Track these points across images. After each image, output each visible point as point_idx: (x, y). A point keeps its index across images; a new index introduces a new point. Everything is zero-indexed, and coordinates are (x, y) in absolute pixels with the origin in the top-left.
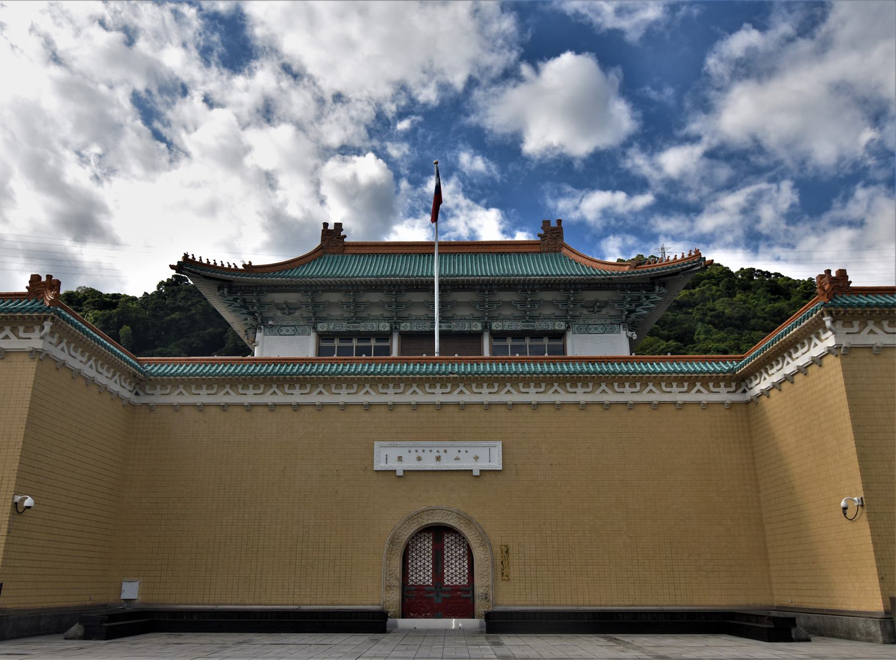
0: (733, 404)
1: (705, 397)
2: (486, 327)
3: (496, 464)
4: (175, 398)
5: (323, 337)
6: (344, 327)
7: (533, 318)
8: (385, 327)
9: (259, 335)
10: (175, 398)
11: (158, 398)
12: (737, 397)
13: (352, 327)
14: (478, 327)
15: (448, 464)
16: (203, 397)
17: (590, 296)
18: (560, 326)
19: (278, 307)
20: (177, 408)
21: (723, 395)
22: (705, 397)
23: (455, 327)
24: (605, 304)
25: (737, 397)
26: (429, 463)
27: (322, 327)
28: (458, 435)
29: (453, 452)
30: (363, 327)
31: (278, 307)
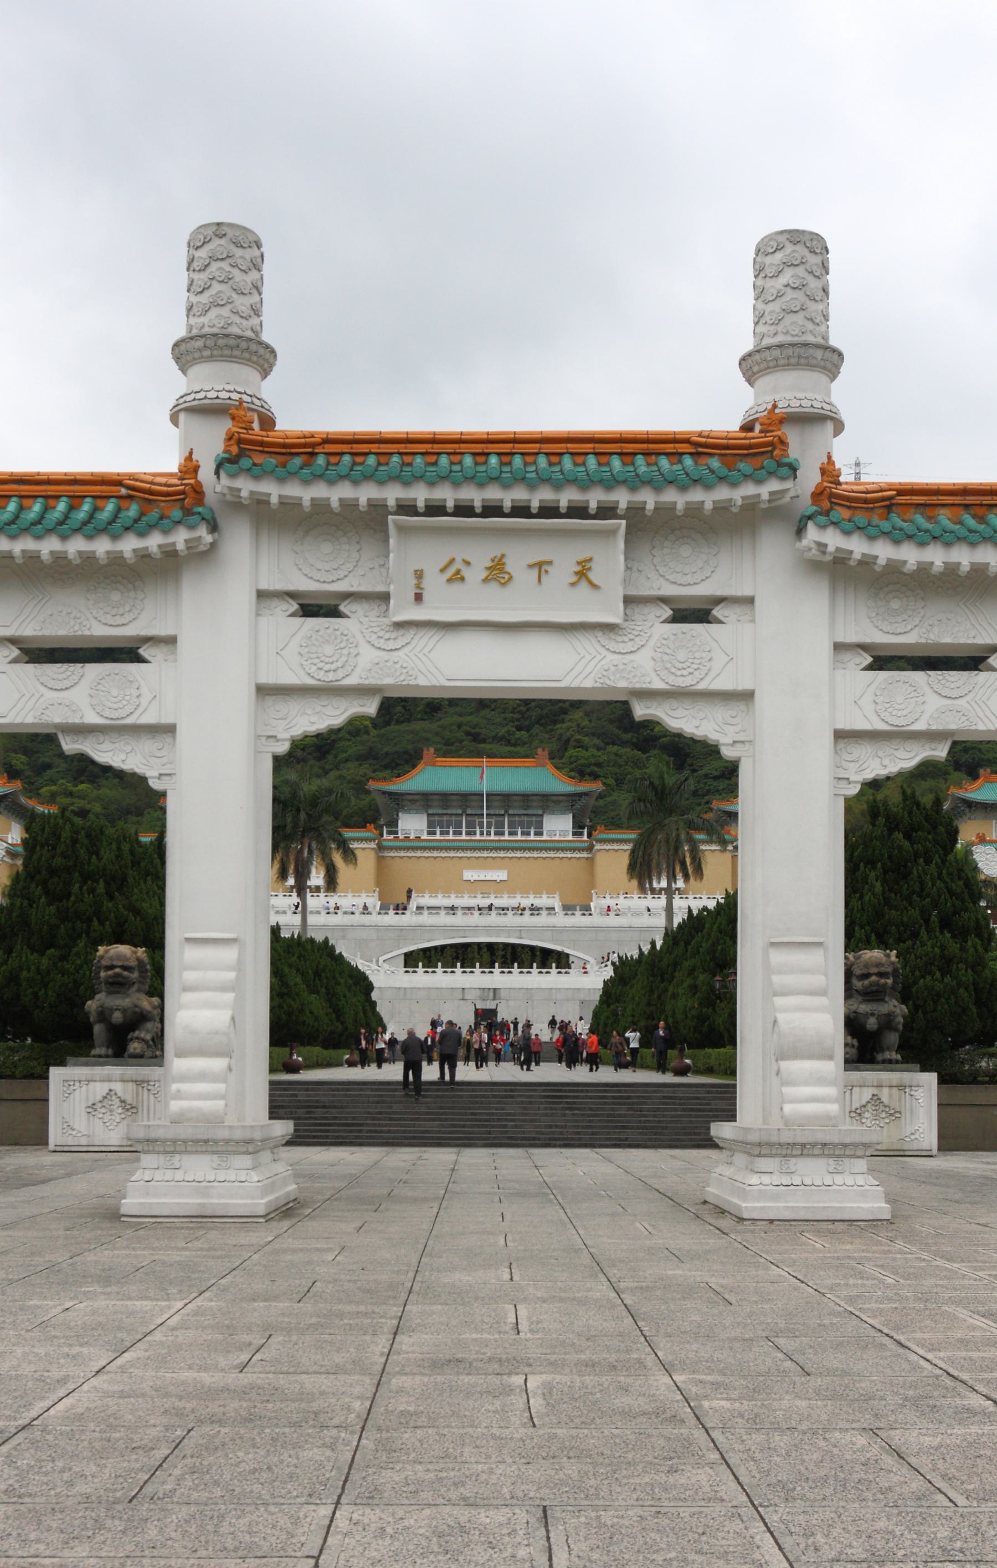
0: (587, 858)
1: (579, 855)
2: (506, 812)
3: (505, 878)
4: (392, 854)
5: (429, 815)
6: (440, 811)
7: (528, 808)
8: (460, 811)
9: (400, 814)
10: (392, 854)
11: (386, 854)
12: (590, 856)
13: (445, 811)
14: (502, 812)
15: (488, 878)
16: (402, 854)
17: (554, 798)
18: (540, 812)
19: (410, 801)
20: (393, 858)
21: (585, 855)
22: (579, 855)
23: (492, 812)
24: (560, 802)
25: (590, 856)
26: (482, 878)
27: (430, 811)
28: (492, 868)
29: (490, 874)
30: (449, 811)
31: (410, 801)
